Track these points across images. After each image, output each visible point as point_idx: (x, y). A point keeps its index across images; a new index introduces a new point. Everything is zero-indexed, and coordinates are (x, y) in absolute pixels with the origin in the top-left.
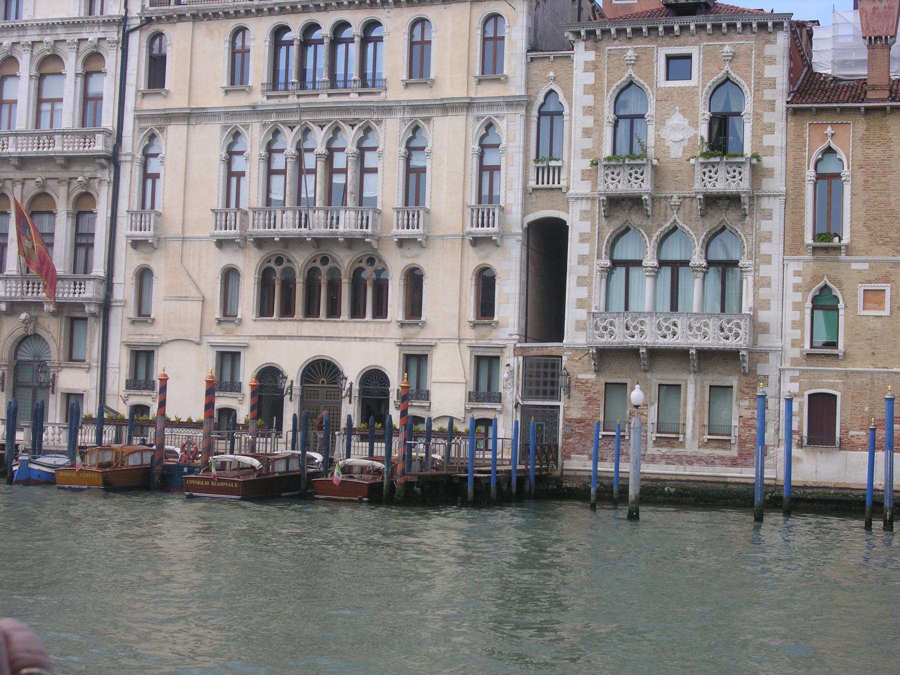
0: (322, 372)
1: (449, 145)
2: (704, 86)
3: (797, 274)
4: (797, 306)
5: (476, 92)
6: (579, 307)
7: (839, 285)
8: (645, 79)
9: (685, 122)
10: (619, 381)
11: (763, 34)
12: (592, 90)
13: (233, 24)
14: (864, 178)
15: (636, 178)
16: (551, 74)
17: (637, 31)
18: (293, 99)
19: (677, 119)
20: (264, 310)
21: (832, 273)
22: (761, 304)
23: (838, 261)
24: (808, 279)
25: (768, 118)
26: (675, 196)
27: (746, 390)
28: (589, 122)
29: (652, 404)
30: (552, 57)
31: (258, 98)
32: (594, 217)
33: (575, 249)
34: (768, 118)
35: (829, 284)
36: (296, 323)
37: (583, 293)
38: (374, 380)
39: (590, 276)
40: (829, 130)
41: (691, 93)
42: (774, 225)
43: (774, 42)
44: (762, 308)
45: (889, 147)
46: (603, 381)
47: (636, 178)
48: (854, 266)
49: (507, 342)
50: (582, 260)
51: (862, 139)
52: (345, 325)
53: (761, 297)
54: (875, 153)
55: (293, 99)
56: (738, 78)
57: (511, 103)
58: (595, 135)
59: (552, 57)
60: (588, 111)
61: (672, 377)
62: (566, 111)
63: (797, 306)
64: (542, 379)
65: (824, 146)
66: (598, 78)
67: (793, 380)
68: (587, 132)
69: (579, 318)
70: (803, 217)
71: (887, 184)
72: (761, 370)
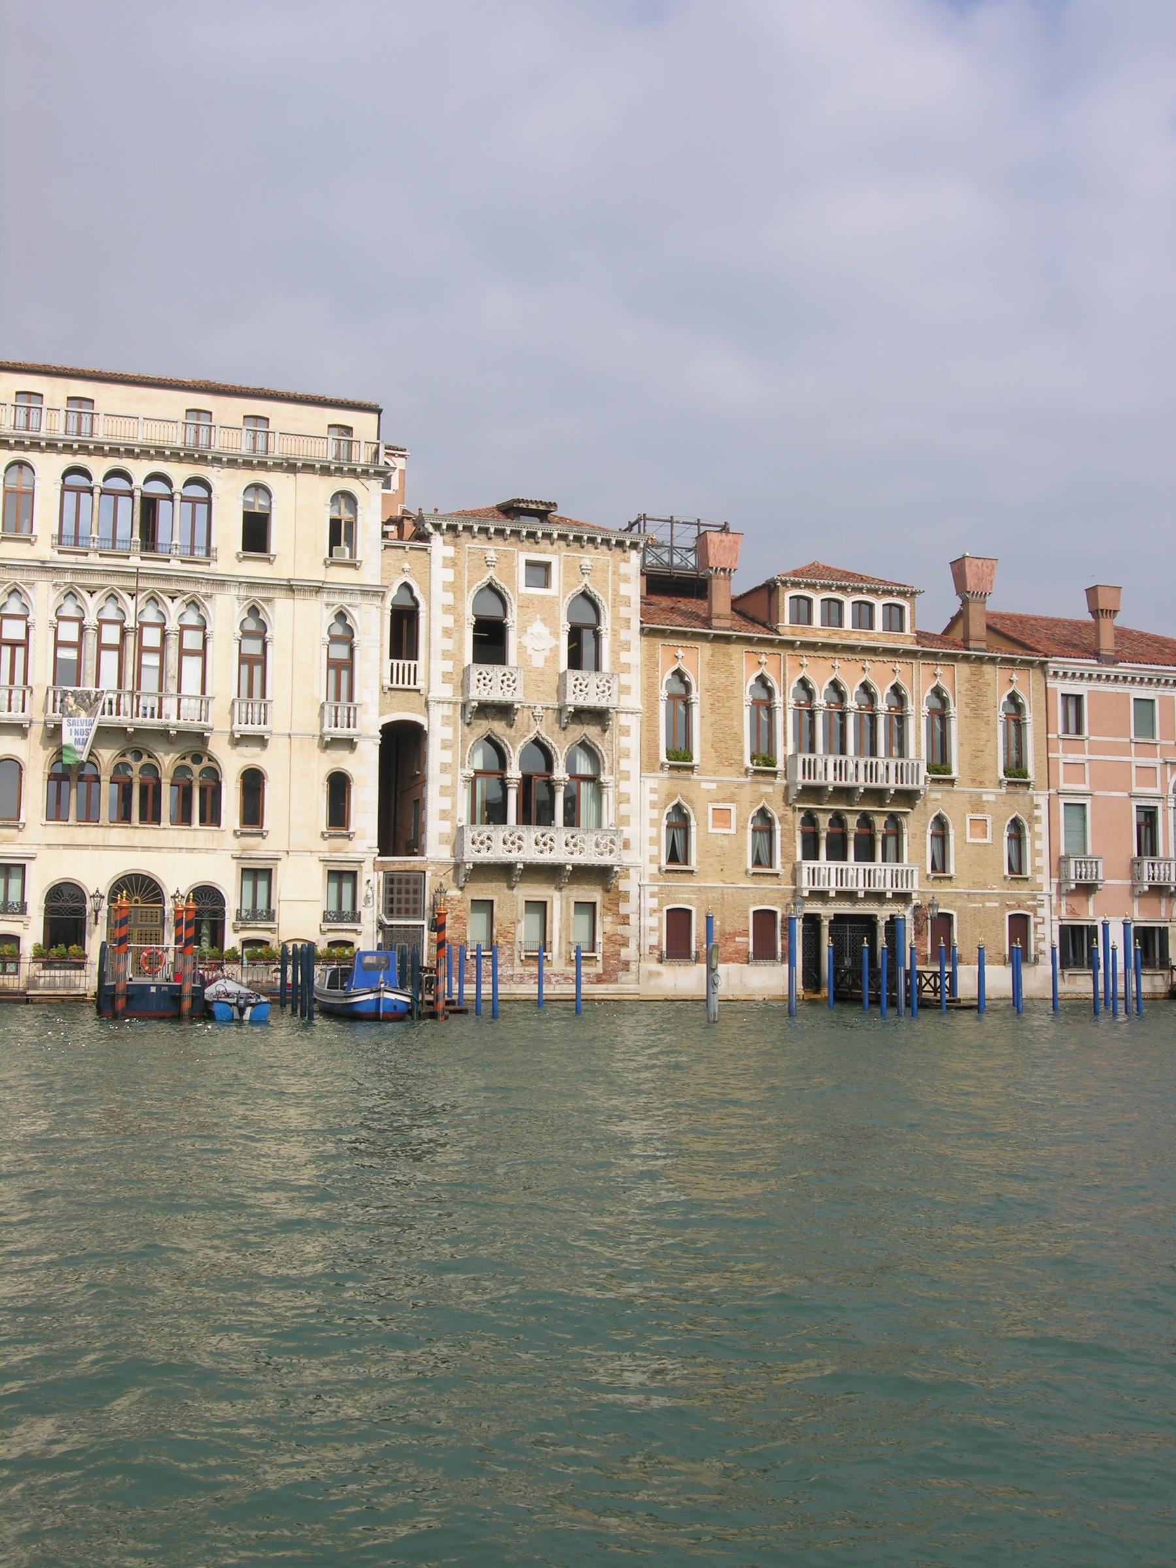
0: (140, 887)
1: (299, 631)
2: (564, 597)
3: (653, 791)
4: (654, 823)
5: (326, 575)
6: (442, 819)
7: (691, 803)
8: (505, 582)
9: (545, 631)
10: (485, 898)
11: (618, 551)
12: (453, 587)
13: (68, 460)
14: (711, 701)
15: (509, 686)
16: (406, 566)
17: (500, 532)
18: (93, 558)
19: (538, 627)
20: (56, 811)
21: (685, 794)
22: (623, 820)
23: (689, 779)
24: (664, 797)
25: (624, 635)
26: (539, 707)
27: (610, 906)
28: (449, 621)
29: (519, 921)
30: (407, 547)
31: (44, 549)
32: (456, 723)
33: (437, 756)
34: (624, 635)
35: (684, 803)
36: (102, 830)
37: (446, 803)
38: (207, 898)
39: (454, 785)
40: (680, 653)
41: (553, 601)
42: (632, 742)
43: (627, 561)
44: (622, 824)
45: (732, 673)
46: (469, 898)
47: (509, 686)
48: (704, 785)
49: (365, 855)
50: (445, 768)
51: (708, 664)
52: (167, 833)
53: (622, 813)
54: (720, 678)
55: (93, 558)
56: (597, 593)
57: (367, 592)
58: (456, 636)
59: (407, 547)
60: (448, 609)
61: (538, 893)
62: (422, 608)
63: (654, 823)
64: (403, 896)
65: (675, 667)
66: (459, 575)
67: (653, 895)
68: (447, 632)
69: (443, 831)
70: (657, 735)
71: (731, 708)
72: (623, 885)
